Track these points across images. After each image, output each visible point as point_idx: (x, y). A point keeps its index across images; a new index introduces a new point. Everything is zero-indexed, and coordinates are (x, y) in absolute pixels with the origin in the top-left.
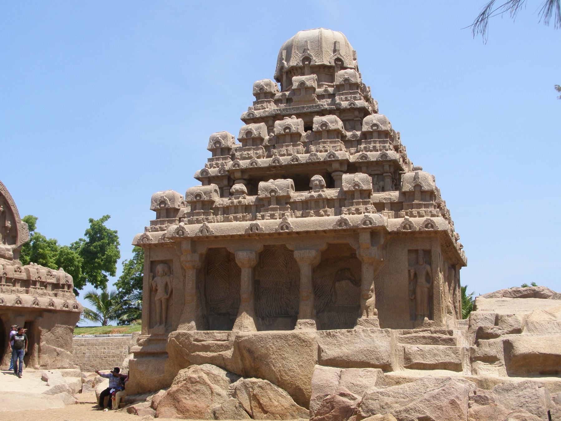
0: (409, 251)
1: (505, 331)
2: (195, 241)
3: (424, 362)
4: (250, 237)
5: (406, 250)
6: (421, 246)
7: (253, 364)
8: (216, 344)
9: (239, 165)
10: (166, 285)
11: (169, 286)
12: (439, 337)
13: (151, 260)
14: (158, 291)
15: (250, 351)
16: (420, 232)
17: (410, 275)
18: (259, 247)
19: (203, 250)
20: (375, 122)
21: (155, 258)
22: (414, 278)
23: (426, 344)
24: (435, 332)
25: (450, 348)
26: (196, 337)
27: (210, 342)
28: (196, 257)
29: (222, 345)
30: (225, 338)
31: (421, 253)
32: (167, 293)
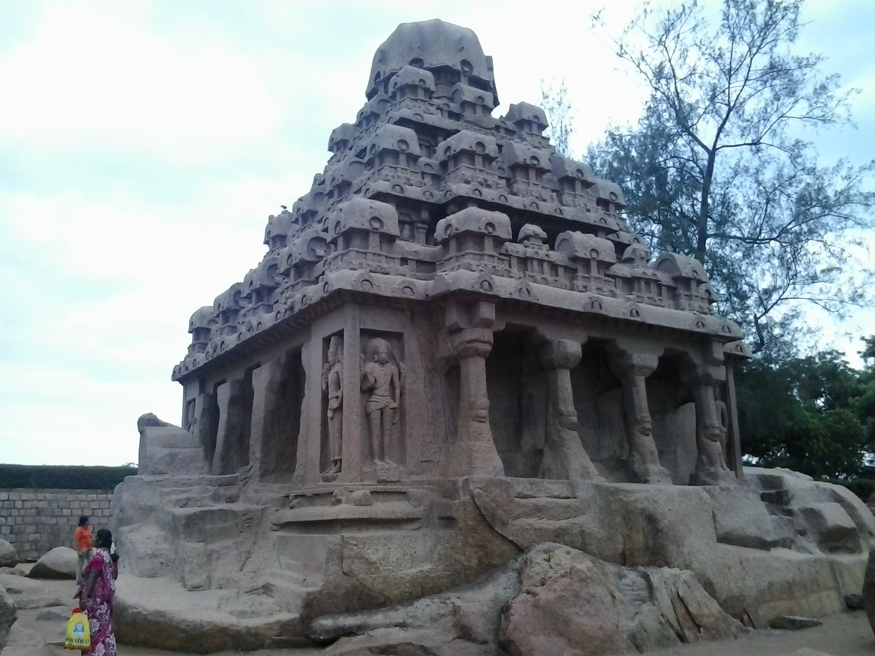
2: (504, 305)
7: (651, 542)
8: (557, 504)
9: (481, 194)
10: (392, 382)
11: (397, 383)
13: (362, 327)
14: (376, 392)
15: (651, 519)
18: (583, 338)
21: (370, 326)
26: (519, 489)
27: (542, 500)
29: (569, 506)
30: (566, 493)
32: (393, 397)
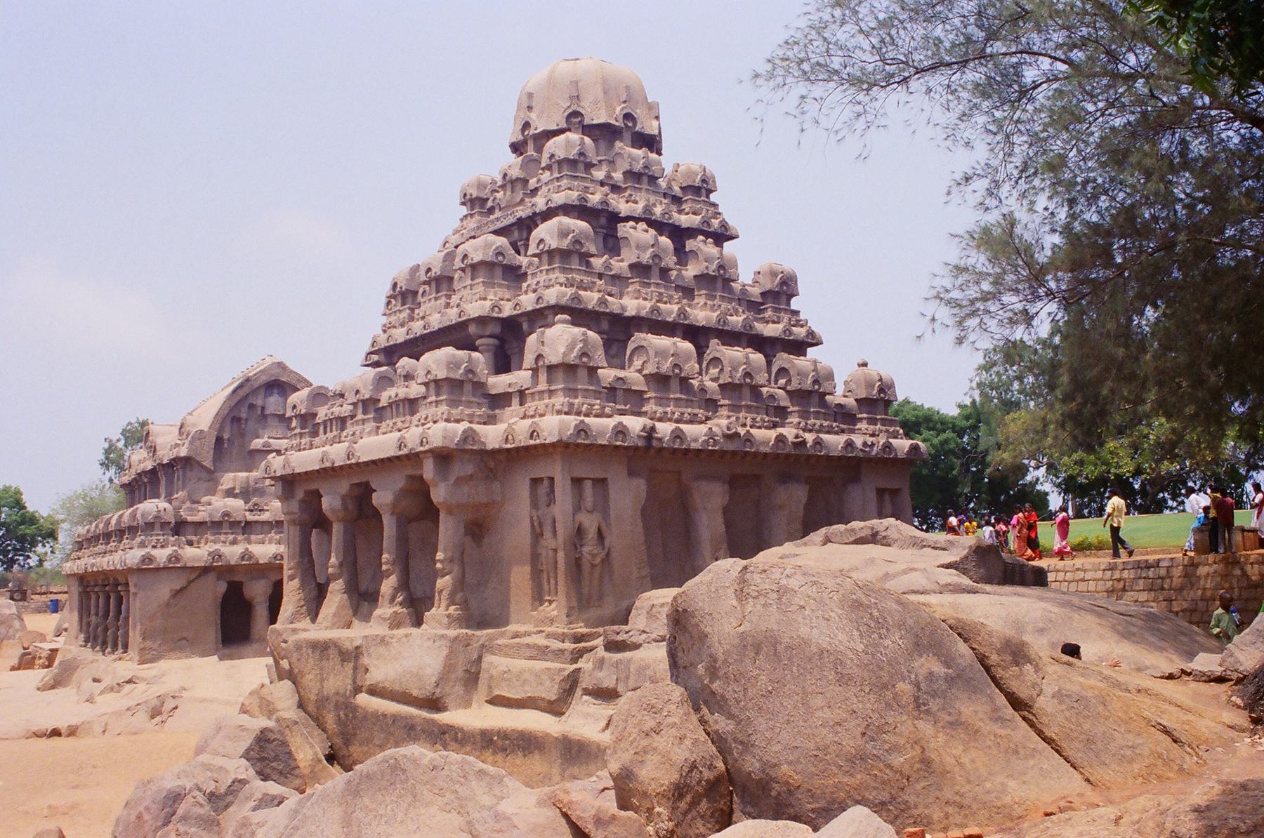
0: (535, 482)
1: (654, 636)
3: (507, 695)
4: (329, 473)
5: (527, 482)
6: (541, 471)
12: (547, 647)
16: (527, 448)
17: (533, 525)
18: (344, 486)
19: (300, 494)
20: (542, 236)
22: (537, 535)
23: (530, 658)
24: (548, 636)
25: (549, 669)
28: (295, 505)
31: (546, 482)
